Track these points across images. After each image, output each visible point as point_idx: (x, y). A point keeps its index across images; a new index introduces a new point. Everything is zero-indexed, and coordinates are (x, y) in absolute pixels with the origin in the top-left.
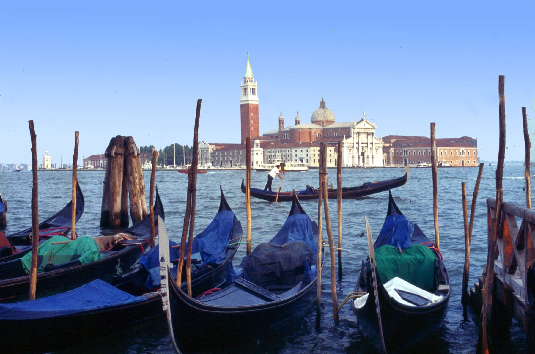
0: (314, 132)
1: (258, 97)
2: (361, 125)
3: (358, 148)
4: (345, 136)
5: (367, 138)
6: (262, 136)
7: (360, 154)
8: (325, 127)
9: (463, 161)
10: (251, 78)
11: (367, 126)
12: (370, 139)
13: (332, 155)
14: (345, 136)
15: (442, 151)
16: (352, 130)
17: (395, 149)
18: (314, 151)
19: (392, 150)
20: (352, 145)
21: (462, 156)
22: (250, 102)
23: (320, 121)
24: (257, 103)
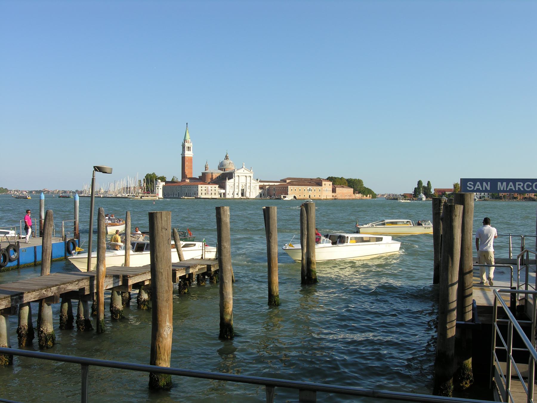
1: (193, 153)
2: (241, 171)
3: (238, 186)
4: (227, 178)
6: (198, 178)
7: (240, 190)
15: (292, 188)
18: (202, 187)
21: (309, 191)
22: (186, 156)
24: (192, 156)
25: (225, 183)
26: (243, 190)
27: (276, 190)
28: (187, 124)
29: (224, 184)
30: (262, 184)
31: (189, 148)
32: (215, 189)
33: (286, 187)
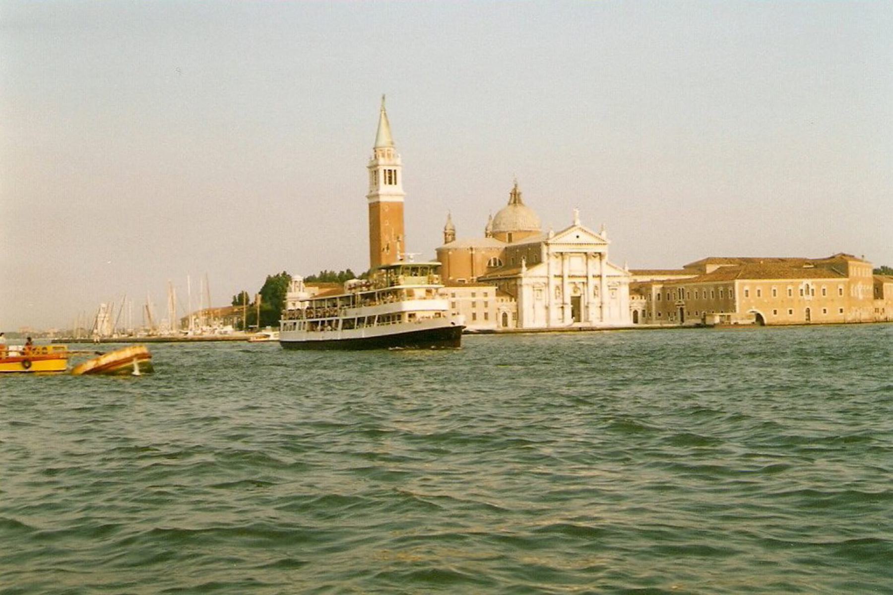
0: (483, 255)
1: (404, 189)
2: (570, 237)
3: (561, 288)
4: (524, 263)
5: (587, 264)
7: (568, 300)
8: (512, 244)
9: (808, 311)
10: (386, 149)
11: (584, 238)
12: (594, 267)
13: (489, 304)
14: (524, 263)
15: (747, 288)
16: (544, 249)
17: (666, 286)
19: (656, 289)
20: (545, 280)
22: (382, 199)
23: (504, 232)
24: (401, 199)
25: (516, 279)
26: (576, 302)
27: (686, 296)
28: (384, 98)
29: (513, 282)
30: (640, 279)
31: (391, 178)
32: (486, 299)
33: (726, 286)
